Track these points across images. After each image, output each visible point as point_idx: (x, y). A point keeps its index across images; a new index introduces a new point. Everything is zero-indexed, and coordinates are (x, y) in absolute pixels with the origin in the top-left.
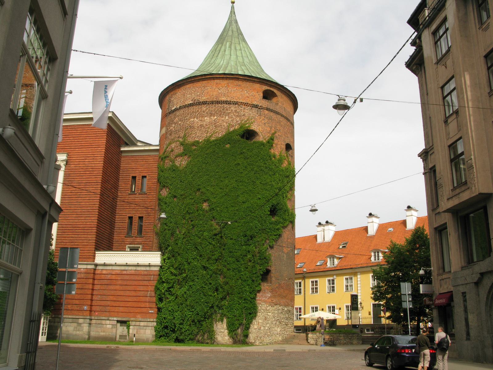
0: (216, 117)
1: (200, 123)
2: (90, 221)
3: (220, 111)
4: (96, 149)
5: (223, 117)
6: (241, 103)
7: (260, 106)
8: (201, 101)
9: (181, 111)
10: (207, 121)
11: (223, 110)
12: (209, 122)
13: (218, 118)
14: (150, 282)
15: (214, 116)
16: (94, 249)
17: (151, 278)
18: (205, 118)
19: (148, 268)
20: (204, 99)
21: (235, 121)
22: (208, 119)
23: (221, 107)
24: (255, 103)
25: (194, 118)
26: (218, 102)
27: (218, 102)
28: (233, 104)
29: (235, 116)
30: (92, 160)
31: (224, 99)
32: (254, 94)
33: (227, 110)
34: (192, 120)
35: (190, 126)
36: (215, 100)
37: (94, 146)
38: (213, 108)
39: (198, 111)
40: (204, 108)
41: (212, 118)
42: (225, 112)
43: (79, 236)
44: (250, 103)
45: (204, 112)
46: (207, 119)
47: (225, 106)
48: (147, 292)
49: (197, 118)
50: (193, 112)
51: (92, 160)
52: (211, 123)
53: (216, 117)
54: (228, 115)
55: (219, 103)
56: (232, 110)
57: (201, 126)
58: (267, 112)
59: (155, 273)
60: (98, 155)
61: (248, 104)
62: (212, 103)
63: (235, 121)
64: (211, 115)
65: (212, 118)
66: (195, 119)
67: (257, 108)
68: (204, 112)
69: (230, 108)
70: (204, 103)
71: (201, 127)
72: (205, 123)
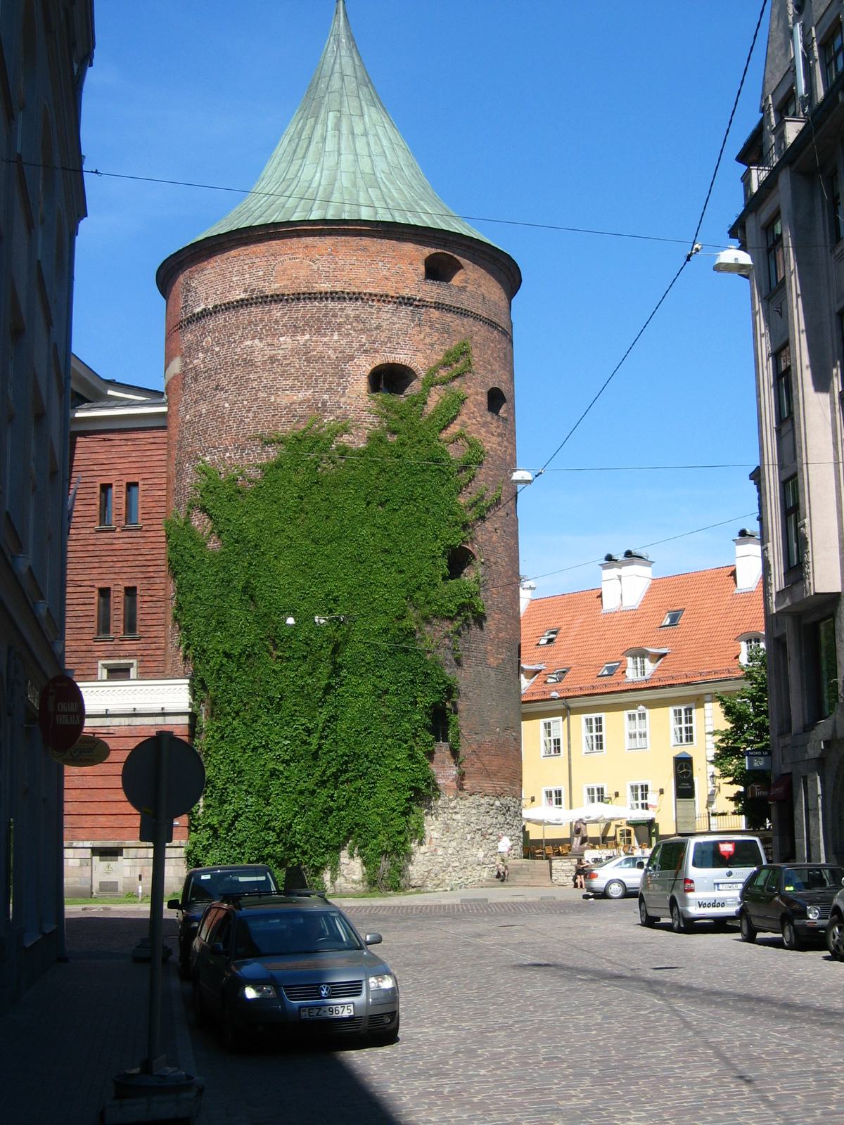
0: (307, 337)
1: (269, 352)
3: (319, 319)
5: (325, 335)
10: (285, 346)
11: (326, 315)
12: (292, 350)
18: (281, 339)
21: (355, 345)
23: (319, 309)
25: (253, 338)
26: (311, 296)
29: (355, 330)
41: (298, 338)
45: (277, 322)
47: (331, 304)
57: (273, 359)
63: (355, 345)
65: (298, 338)
71: (272, 363)
72: (281, 352)
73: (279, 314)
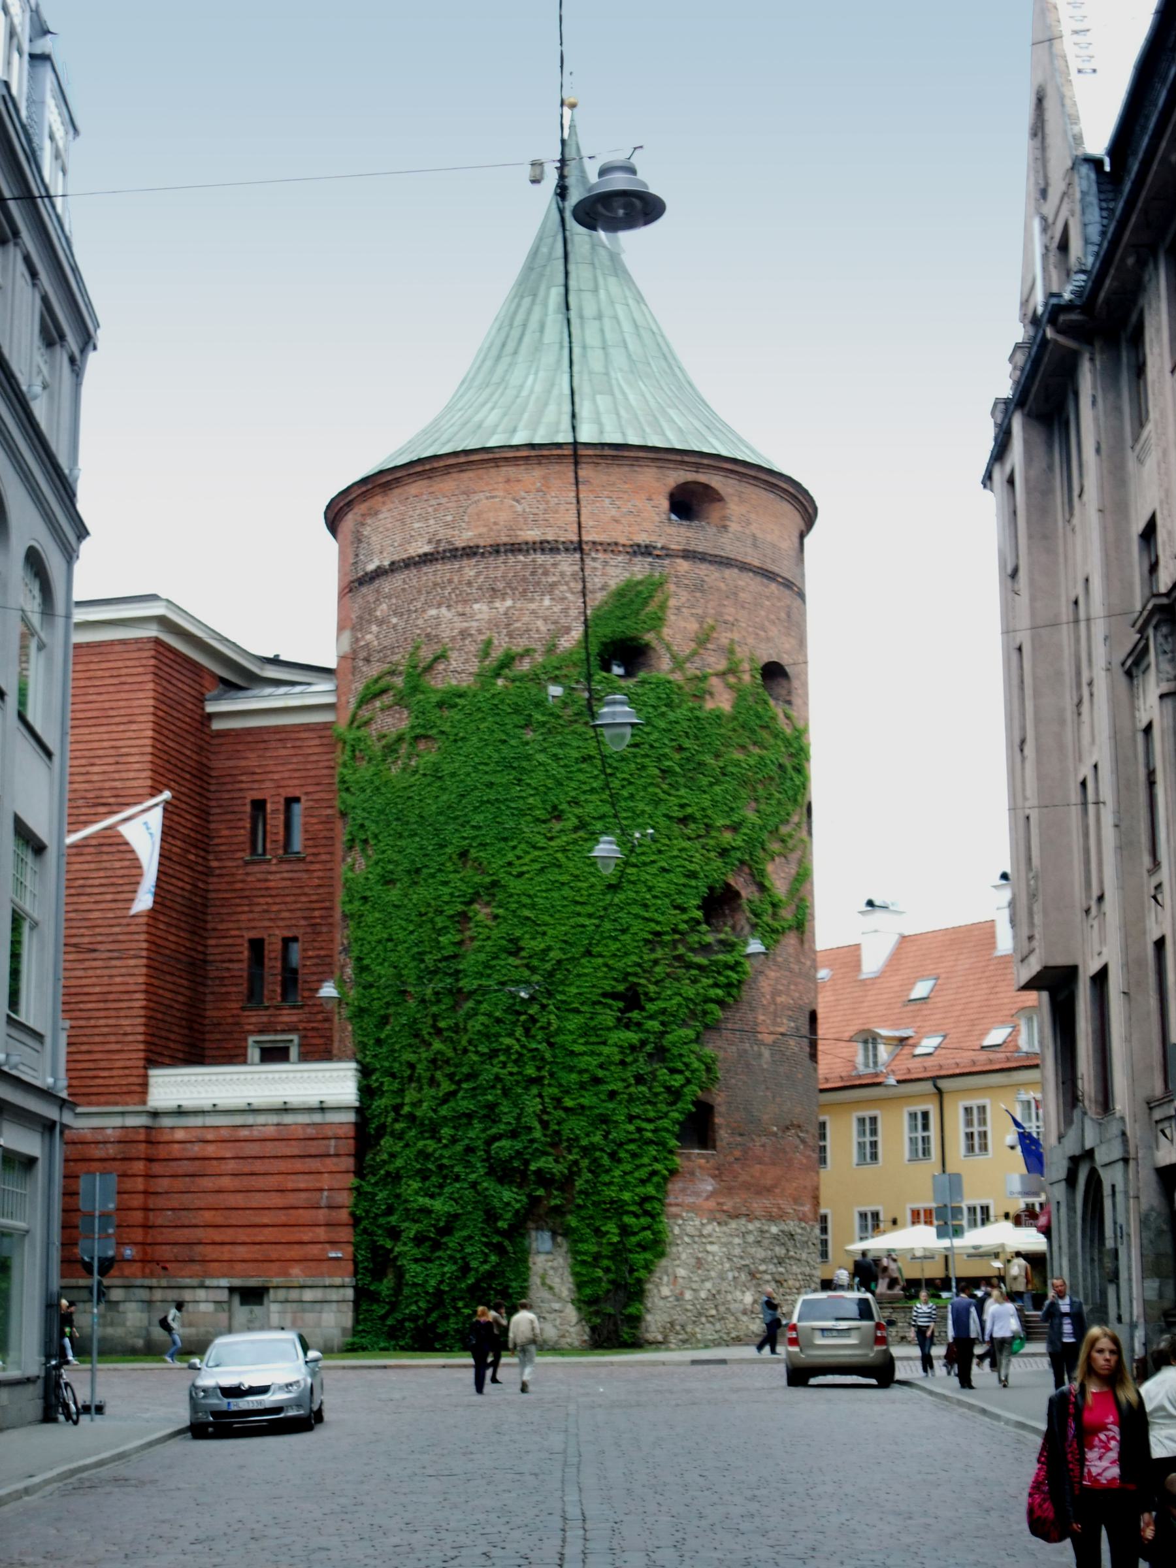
0: (509, 603)
1: (460, 625)
2: (123, 971)
3: (524, 579)
4: (122, 728)
5: (532, 600)
6: (594, 543)
7: (662, 548)
8: (459, 544)
9: (396, 581)
11: (533, 573)
13: (518, 605)
14: (328, 1161)
15: (504, 599)
16: (141, 1063)
17: (328, 1146)
18: (476, 606)
19: (317, 1118)
20: (464, 537)
22: (485, 608)
23: (525, 565)
24: (642, 539)
25: (439, 606)
26: (515, 548)
27: (515, 548)
28: (567, 550)
30: (112, 768)
31: (532, 534)
32: (634, 510)
33: (546, 573)
34: (433, 612)
35: (428, 635)
36: (505, 539)
37: (117, 720)
38: (500, 568)
39: (450, 581)
40: (469, 569)
41: (497, 605)
42: (538, 583)
43: (92, 1022)
44: (622, 540)
45: (469, 584)
46: (481, 609)
47: (540, 558)
48: (318, 1194)
49: (449, 607)
50: (436, 584)
51: (112, 768)
52: (494, 624)
53: (509, 603)
54: (551, 592)
55: (520, 550)
56: (562, 574)
57: (464, 634)
58: (683, 565)
59: (341, 1132)
60: (133, 750)
61: (616, 544)
62: (496, 550)
64: (495, 593)
65: (497, 605)
66: (444, 610)
67: (650, 554)
68: (469, 584)
69: (554, 565)
70: (470, 552)
72: (474, 624)
73: (472, 573)
